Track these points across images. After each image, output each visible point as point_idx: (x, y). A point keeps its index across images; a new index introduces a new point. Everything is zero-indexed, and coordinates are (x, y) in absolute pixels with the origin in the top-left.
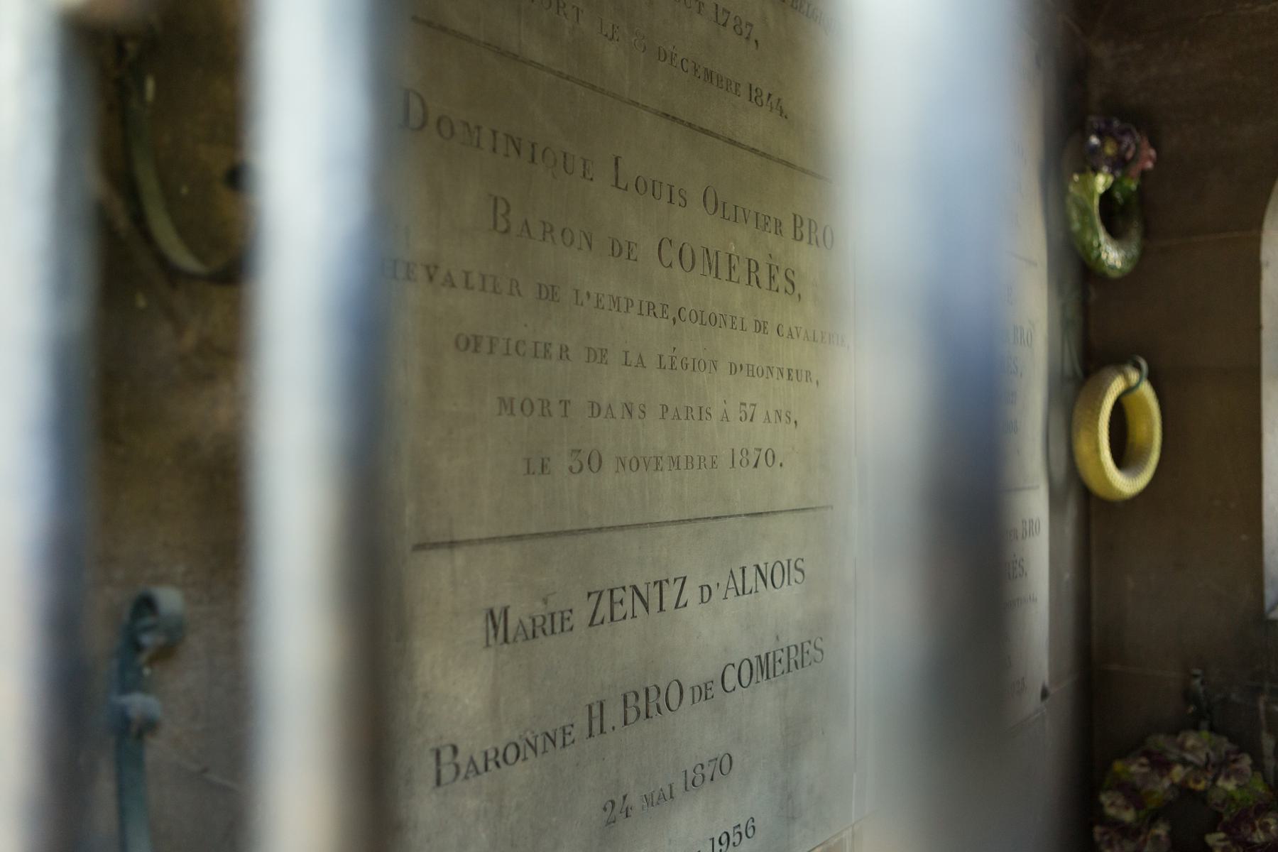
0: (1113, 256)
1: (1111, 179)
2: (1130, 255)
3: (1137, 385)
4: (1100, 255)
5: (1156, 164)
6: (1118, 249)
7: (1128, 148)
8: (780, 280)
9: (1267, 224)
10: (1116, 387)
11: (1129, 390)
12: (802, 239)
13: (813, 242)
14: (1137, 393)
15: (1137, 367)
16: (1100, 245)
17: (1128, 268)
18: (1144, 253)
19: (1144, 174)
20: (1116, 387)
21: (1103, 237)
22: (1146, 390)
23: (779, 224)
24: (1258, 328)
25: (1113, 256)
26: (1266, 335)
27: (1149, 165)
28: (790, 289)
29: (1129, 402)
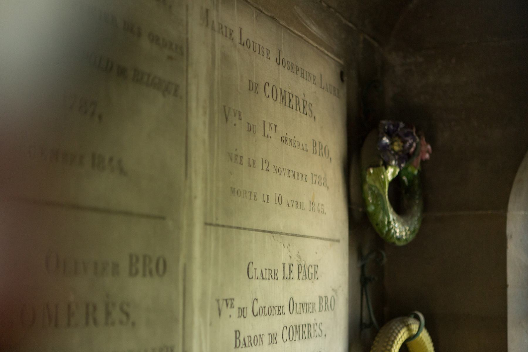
0: (399, 229)
1: (398, 170)
2: (412, 229)
3: (417, 334)
4: (390, 230)
5: (430, 155)
6: (403, 225)
7: (411, 145)
8: (116, 314)
9: (510, 206)
10: (402, 336)
11: (411, 338)
12: (137, 272)
13: (147, 273)
14: (417, 339)
15: (417, 318)
16: (389, 223)
17: (411, 238)
18: (424, 222)
19: (423, 162)
20: (402, 336)
21: (392, 216)
22: (425, 336)
23: (116, 266)
24: (505, 286)
25: (399, 229)
26: (510, 292)
27: (427, 156)
28: (124, 318)
29: (410, 344)
